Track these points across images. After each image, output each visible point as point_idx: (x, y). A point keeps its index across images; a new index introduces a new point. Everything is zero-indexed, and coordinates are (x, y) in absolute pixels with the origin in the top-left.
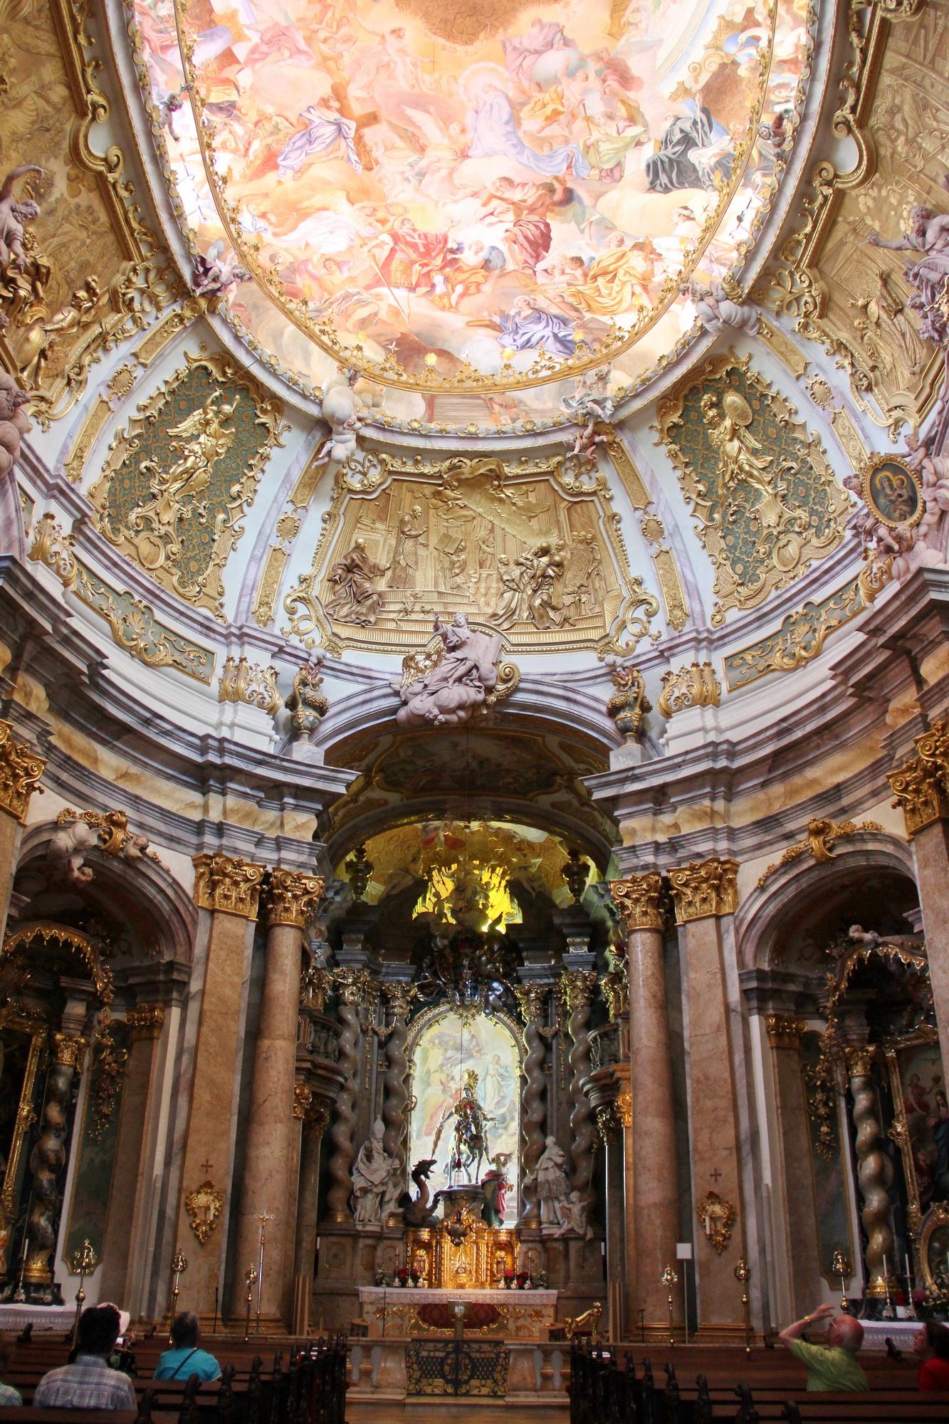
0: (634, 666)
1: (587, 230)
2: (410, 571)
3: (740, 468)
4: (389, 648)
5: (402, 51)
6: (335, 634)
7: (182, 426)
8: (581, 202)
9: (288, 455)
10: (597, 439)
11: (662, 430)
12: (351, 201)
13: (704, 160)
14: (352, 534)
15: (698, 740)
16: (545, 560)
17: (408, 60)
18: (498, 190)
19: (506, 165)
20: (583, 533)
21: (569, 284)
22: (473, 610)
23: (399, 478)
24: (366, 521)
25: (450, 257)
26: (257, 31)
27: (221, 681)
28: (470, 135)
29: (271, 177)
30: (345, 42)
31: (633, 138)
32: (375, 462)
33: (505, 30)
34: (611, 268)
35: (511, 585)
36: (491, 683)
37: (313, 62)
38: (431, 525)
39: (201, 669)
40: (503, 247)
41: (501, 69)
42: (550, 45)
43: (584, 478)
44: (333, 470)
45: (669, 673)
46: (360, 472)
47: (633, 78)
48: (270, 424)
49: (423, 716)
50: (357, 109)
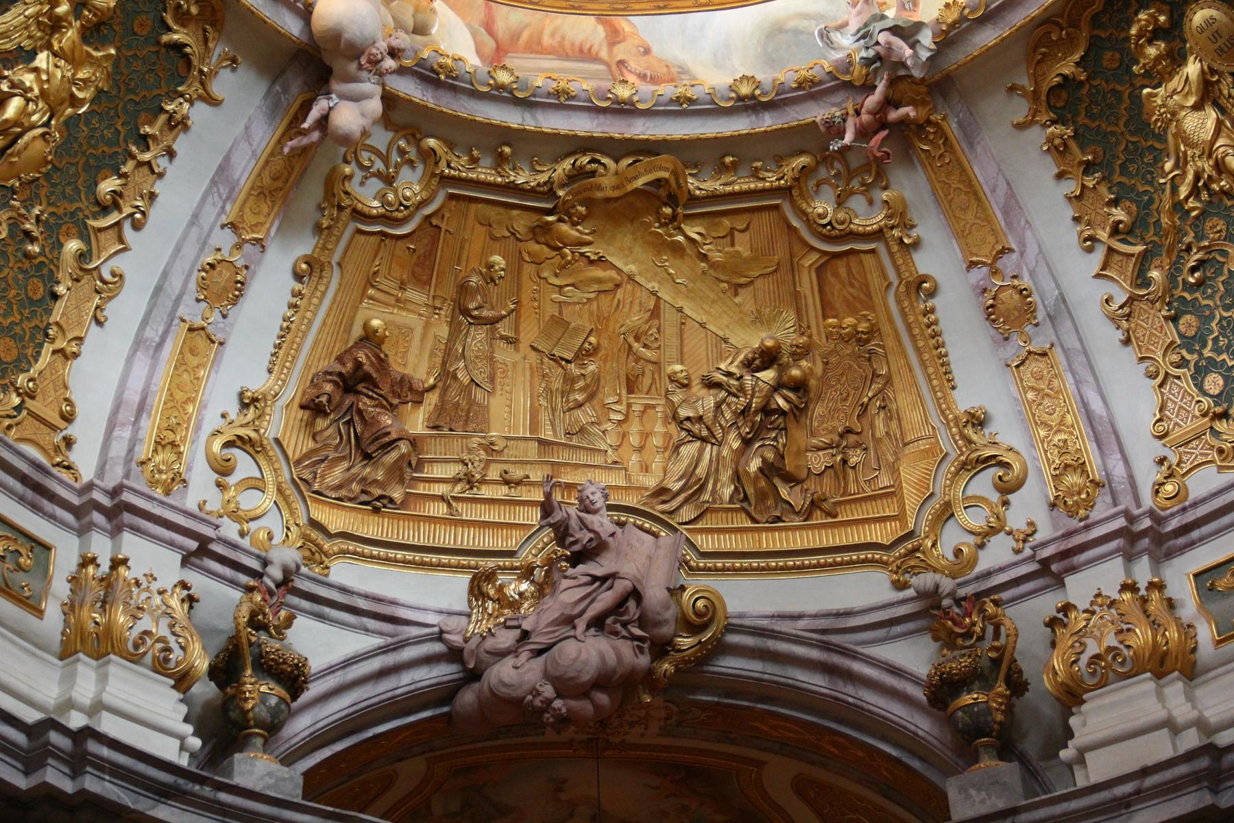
0: (978, 596)
2: (479, 395)
4: (435, 558)
6: (314, 524)
10: (893, 115)
11: (1035, 95)
14: (356, 309)
15: (1160, 748)
16: (768, 375)
20: (850, 320)
22: (616, 479)
23: (461, 193)
24: (386, 284)
27: (70, 608)
32: (413, 154)
35: (696, 430)
36: (667, 630)
38: (525, 298)
39: (22, 579)
43: (857, 203)
44: (320, 169)
45: (1067, 608)
46: (378, 175)
48: (193, 49)
49: (516, 703)
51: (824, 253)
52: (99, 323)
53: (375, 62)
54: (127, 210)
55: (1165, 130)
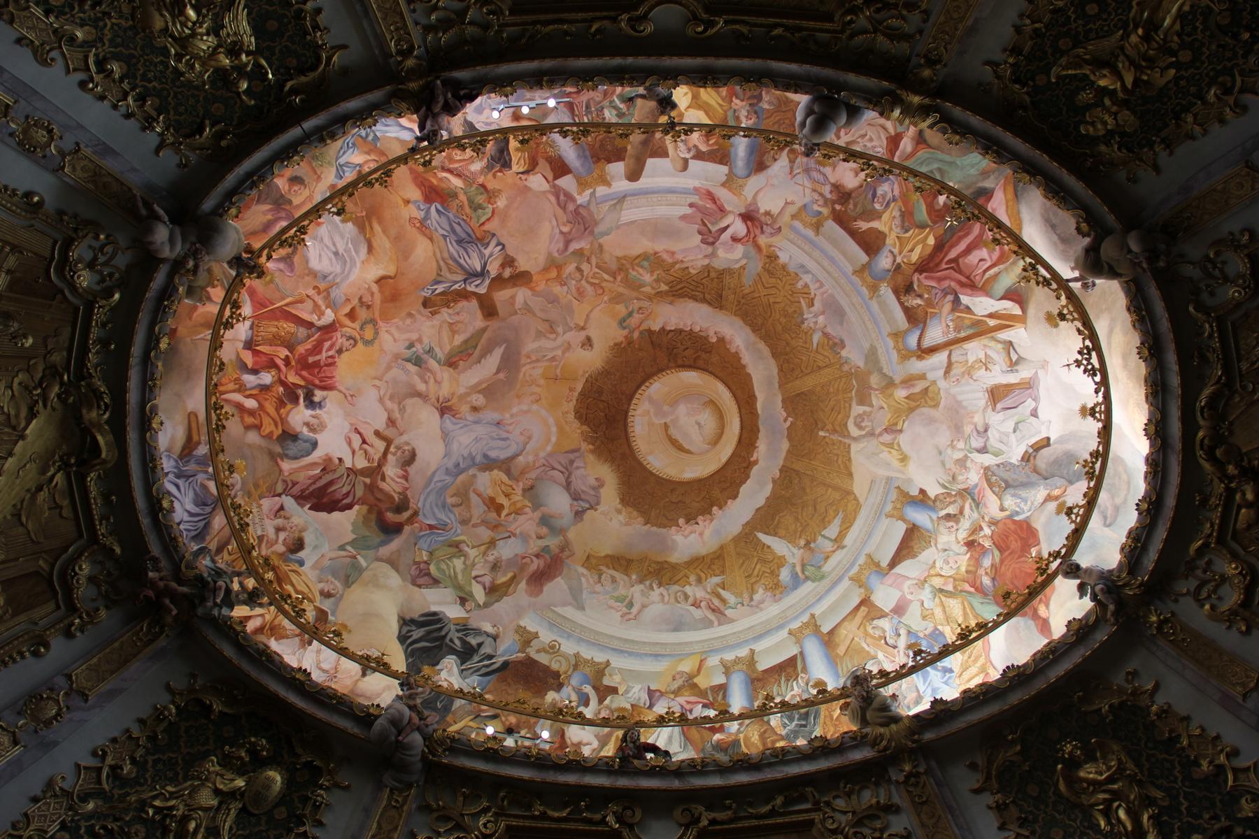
1: (343, 553)
3: (185, 819)
5: (568, 347)
7: (243, 15)
8: (383, 543)
9: (144, 157)
12: (380, 281)
13: (444, 675)
17: (559, 352)
18: (398, 448)
19: (431, 453)
21: (261, 538)
25: (301, 393)
26: (589, 201)
28: (470, 417)
29: (415, 194)
30: (578, 289)
31: (471, 595)
32: (108, 283)
33: (592, 452)
34: (289, 588)
37: (556, 254)
40: (317, 455)
41: (549, 448)
42: (576, 497)
46: (95, 258)
47: (542, 585)
50: (501, 296)
51: (51, 574)
52: (19, 41)
53: (195, 254)
54: (97, 78)
55: (193, 779)
